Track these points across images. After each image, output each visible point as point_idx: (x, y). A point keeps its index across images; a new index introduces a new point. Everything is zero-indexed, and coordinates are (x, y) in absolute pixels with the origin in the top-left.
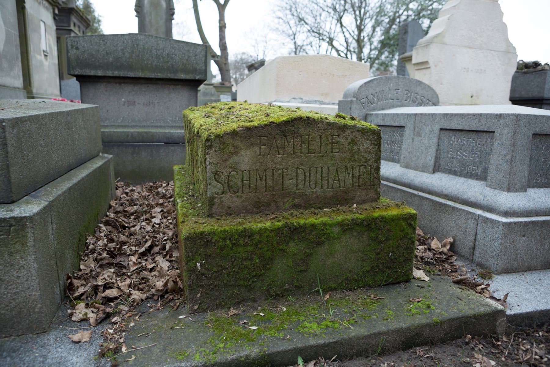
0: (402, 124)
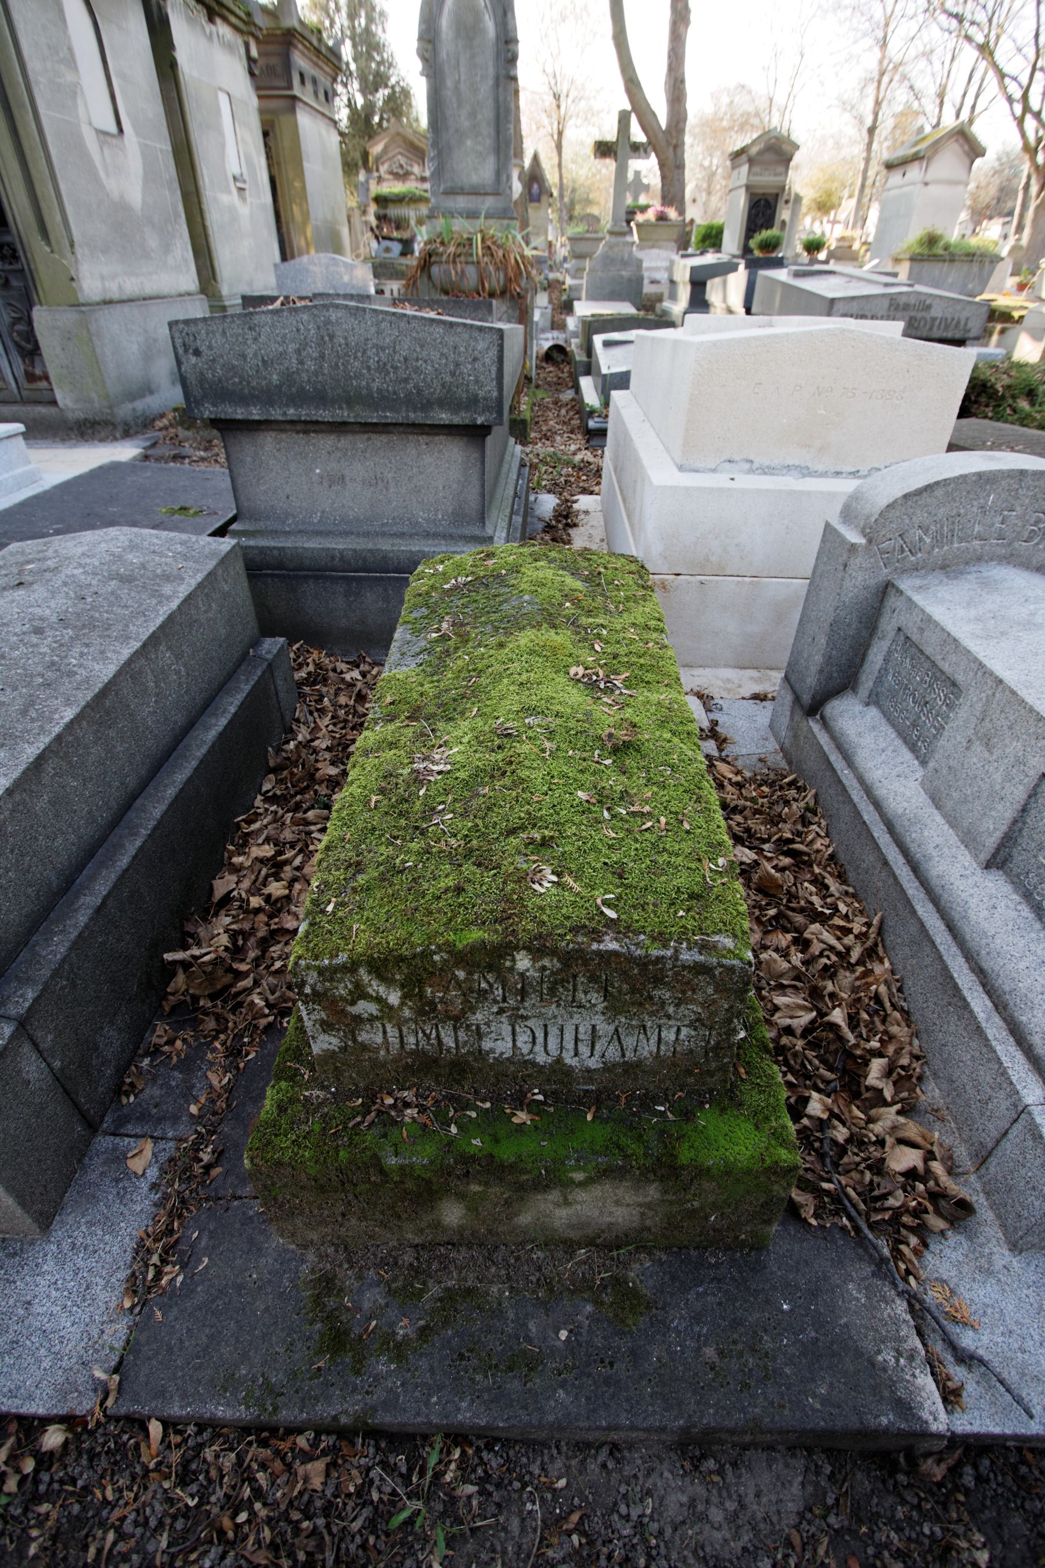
0: (960, 678)
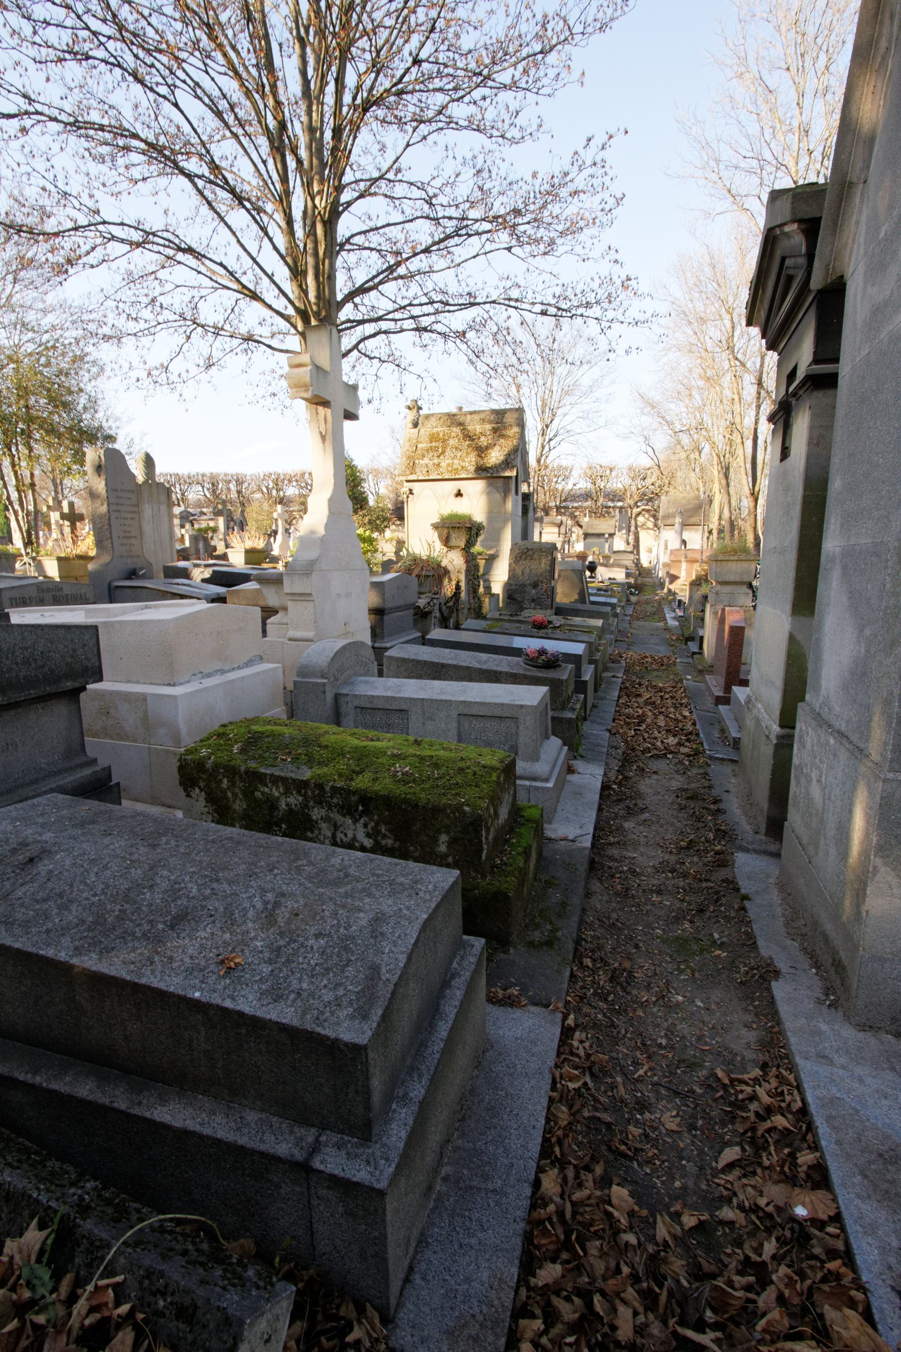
0: (404, 707)
